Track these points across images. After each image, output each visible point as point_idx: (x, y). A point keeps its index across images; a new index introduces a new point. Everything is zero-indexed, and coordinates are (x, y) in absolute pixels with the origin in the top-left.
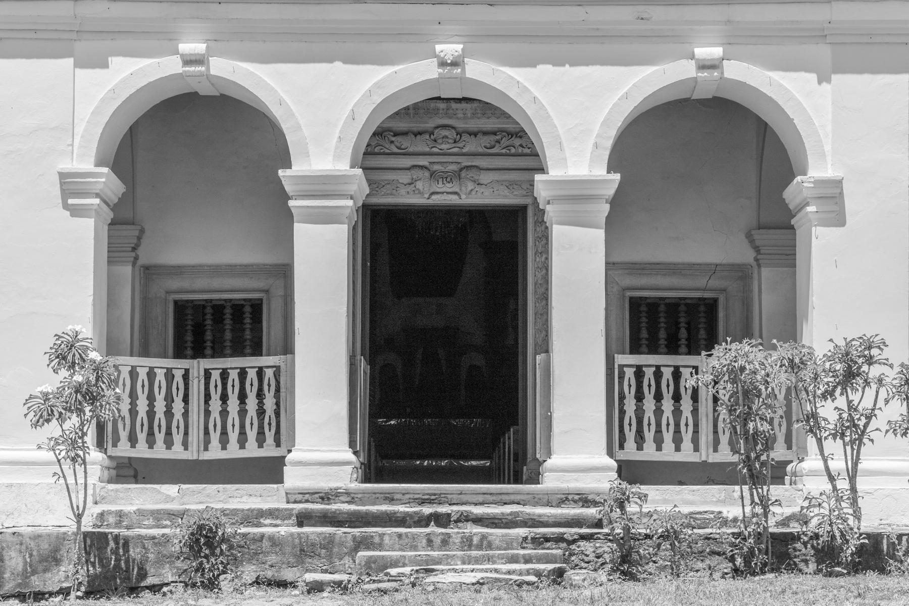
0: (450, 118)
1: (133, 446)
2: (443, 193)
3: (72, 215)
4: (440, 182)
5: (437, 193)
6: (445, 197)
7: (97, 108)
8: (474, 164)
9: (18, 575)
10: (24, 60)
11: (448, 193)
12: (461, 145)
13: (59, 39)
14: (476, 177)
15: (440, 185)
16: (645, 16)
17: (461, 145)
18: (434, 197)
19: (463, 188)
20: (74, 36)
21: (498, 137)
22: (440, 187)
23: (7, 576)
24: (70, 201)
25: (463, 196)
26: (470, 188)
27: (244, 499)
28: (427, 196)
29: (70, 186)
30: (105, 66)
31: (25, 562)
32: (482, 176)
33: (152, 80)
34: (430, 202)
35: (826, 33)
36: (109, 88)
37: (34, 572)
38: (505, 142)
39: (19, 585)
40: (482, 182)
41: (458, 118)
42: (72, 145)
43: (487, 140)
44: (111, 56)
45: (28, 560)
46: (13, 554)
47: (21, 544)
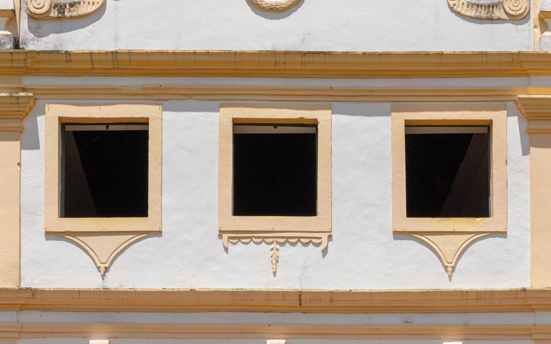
13: (7, 338)
16: (409, 320)
20: (17, 335)
35: (532, 332)
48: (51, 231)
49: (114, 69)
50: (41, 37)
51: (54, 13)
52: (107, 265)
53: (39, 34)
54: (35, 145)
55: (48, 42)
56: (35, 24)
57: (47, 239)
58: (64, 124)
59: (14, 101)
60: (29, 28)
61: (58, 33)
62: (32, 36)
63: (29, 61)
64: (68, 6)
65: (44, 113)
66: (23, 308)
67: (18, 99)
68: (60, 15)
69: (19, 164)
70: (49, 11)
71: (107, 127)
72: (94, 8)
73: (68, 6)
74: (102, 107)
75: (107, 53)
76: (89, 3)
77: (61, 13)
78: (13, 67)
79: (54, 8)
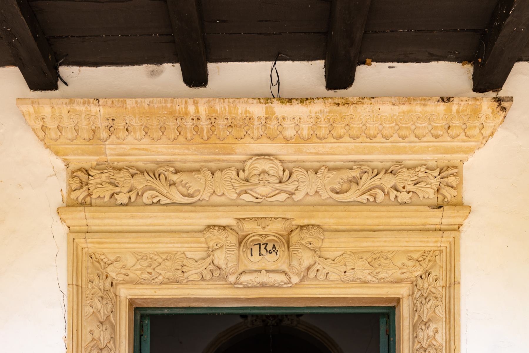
0: (272, 139)
8: (313, 222)
11: (267, 271)
12: (290, 187)
14: (317, 244)
17: (290, 187)
19: (295, 263)
21: (355, 173)
22: (256, 261)
25: (295, 279)
26: (306, 263)
32: (326, 244)
38: (367, 182)
40: (325, 254)
41: (287, 140)
43: (336, 180)
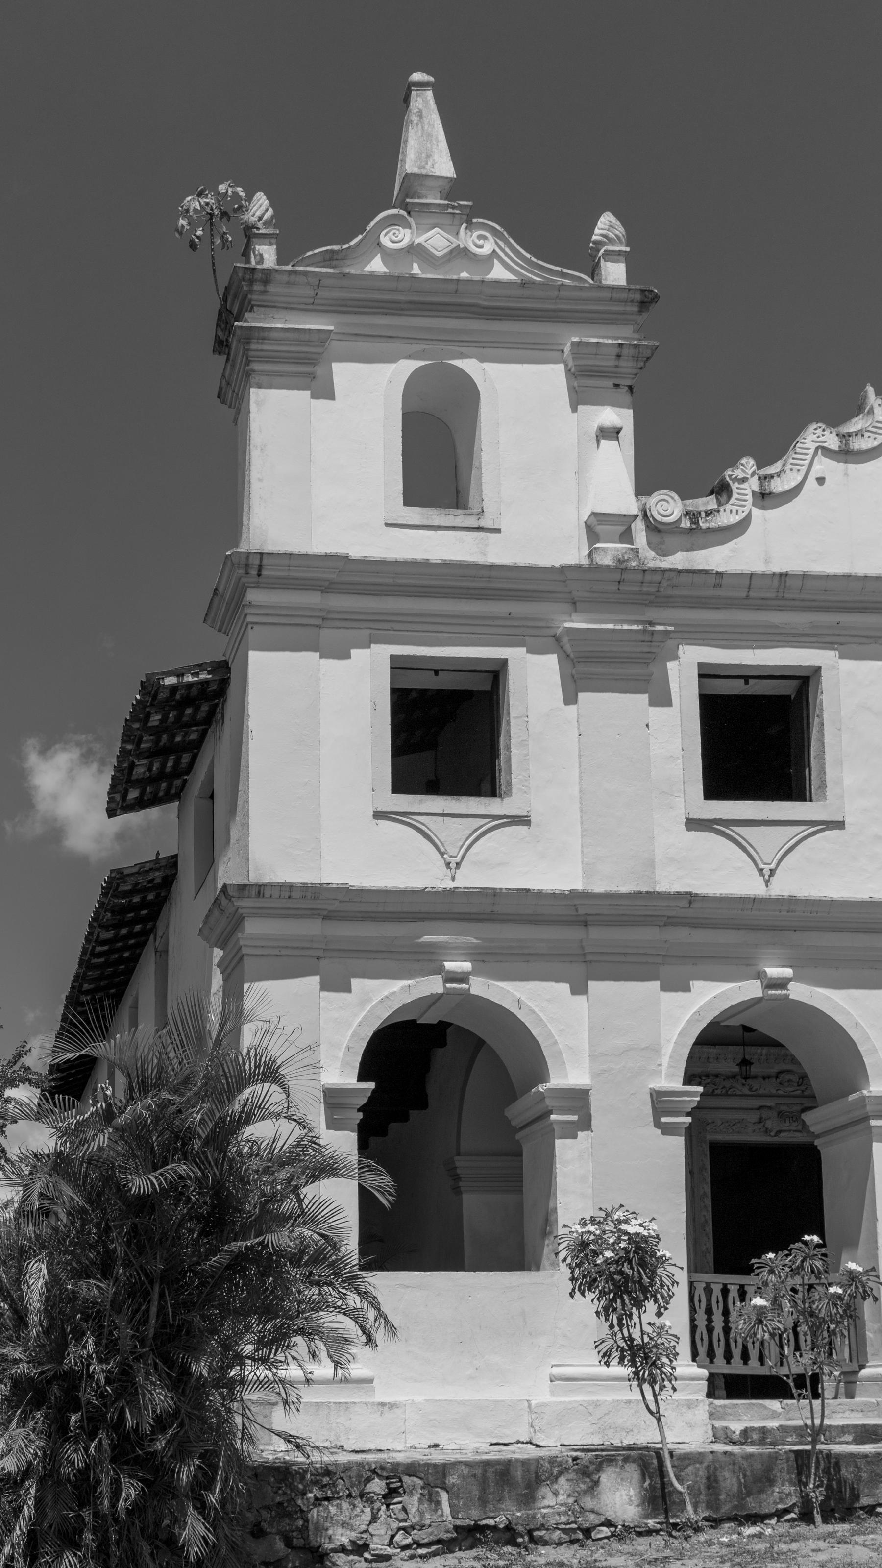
1: (745, 1363)
2: (790, 1131)
3: (663, 1134)
4: (787, 1122)
5: (785, 1131)
6: (791, 1134)
7: (683, 1029)
9: (734, 1496)
10: (612, 983)
15: (788, 1123)
18: (782, 1134)
22: (785, 1126)
23: (722, 1497)
24: (664, 1120)
27: (847, 1414)
28: (772, 1134)
29: (661, 1103)
30: (687, 989)
31: (740, 1483)
33: (734, 1003)
34: (776, 1139)
36: (694, 1010)
37: (749, 1494)
39: (735, 1507)
42: (660, 1065)
44: (693, 980)
45: (743, 1481)
46: (727, 1474)
47: (734, 1464)
48: (695, 817)
49: (776, 598)
50: (665, 555)
51: (686, 524)
52: (773, 866)
53: (663, 553)
54: (668, 703)
55: (678, 560)
56: (656, 538)
57: (688, 830)
58: (706, 674)
59: (647, 637)
60: (649, 544)
61: (688, 551)
62: (653, 554)
63: (665, 584)
64: (703, 515)
65: (676, 657)
66: (670, 922)
67: (653, 634)
68: (694, 526)
69: (647, 725)
70: (679, 520)
71: (747, 683)
72: (738, 518)
73: (703, 515)
74: (757, 651)
75: (774, 574)
76: (731, 511)
77: (695, 524)
78: (641, 593)
79: (685, 516)
